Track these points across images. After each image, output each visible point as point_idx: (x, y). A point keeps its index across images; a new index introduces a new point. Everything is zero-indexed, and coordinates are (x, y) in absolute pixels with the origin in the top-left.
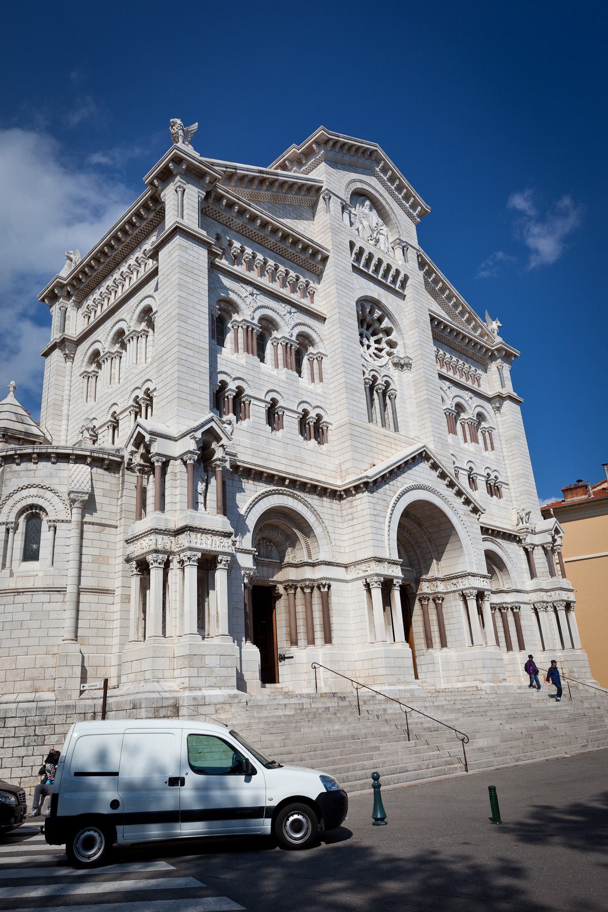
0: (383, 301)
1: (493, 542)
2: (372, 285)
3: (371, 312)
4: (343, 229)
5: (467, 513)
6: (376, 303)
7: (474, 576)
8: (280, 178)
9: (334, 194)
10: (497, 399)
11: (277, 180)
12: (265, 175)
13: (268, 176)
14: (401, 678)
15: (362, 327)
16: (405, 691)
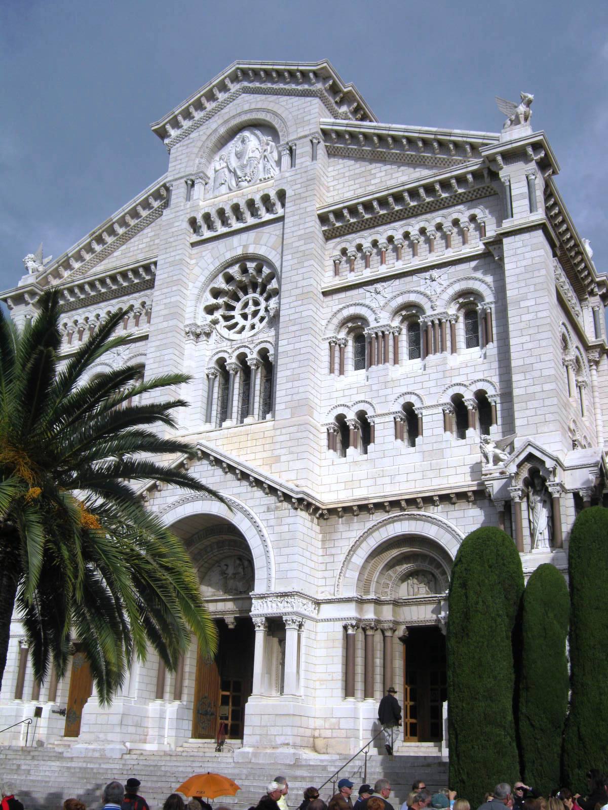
0: (251, 250)
1: (417, 519)
2: (236, 239)
3: (244, 271)
4: (181, 213)
5: (273, 506)
6: (242, 260)
7: (262, 598)
8: (114, 220)
9: (176, 180)
10: (491, 248)
11: (114, 223)
12: (97, 234)
13: (100, 231)
14: (102, 736)
15: (246, 293)
16: (94, 750)
